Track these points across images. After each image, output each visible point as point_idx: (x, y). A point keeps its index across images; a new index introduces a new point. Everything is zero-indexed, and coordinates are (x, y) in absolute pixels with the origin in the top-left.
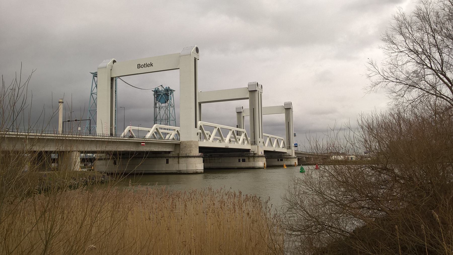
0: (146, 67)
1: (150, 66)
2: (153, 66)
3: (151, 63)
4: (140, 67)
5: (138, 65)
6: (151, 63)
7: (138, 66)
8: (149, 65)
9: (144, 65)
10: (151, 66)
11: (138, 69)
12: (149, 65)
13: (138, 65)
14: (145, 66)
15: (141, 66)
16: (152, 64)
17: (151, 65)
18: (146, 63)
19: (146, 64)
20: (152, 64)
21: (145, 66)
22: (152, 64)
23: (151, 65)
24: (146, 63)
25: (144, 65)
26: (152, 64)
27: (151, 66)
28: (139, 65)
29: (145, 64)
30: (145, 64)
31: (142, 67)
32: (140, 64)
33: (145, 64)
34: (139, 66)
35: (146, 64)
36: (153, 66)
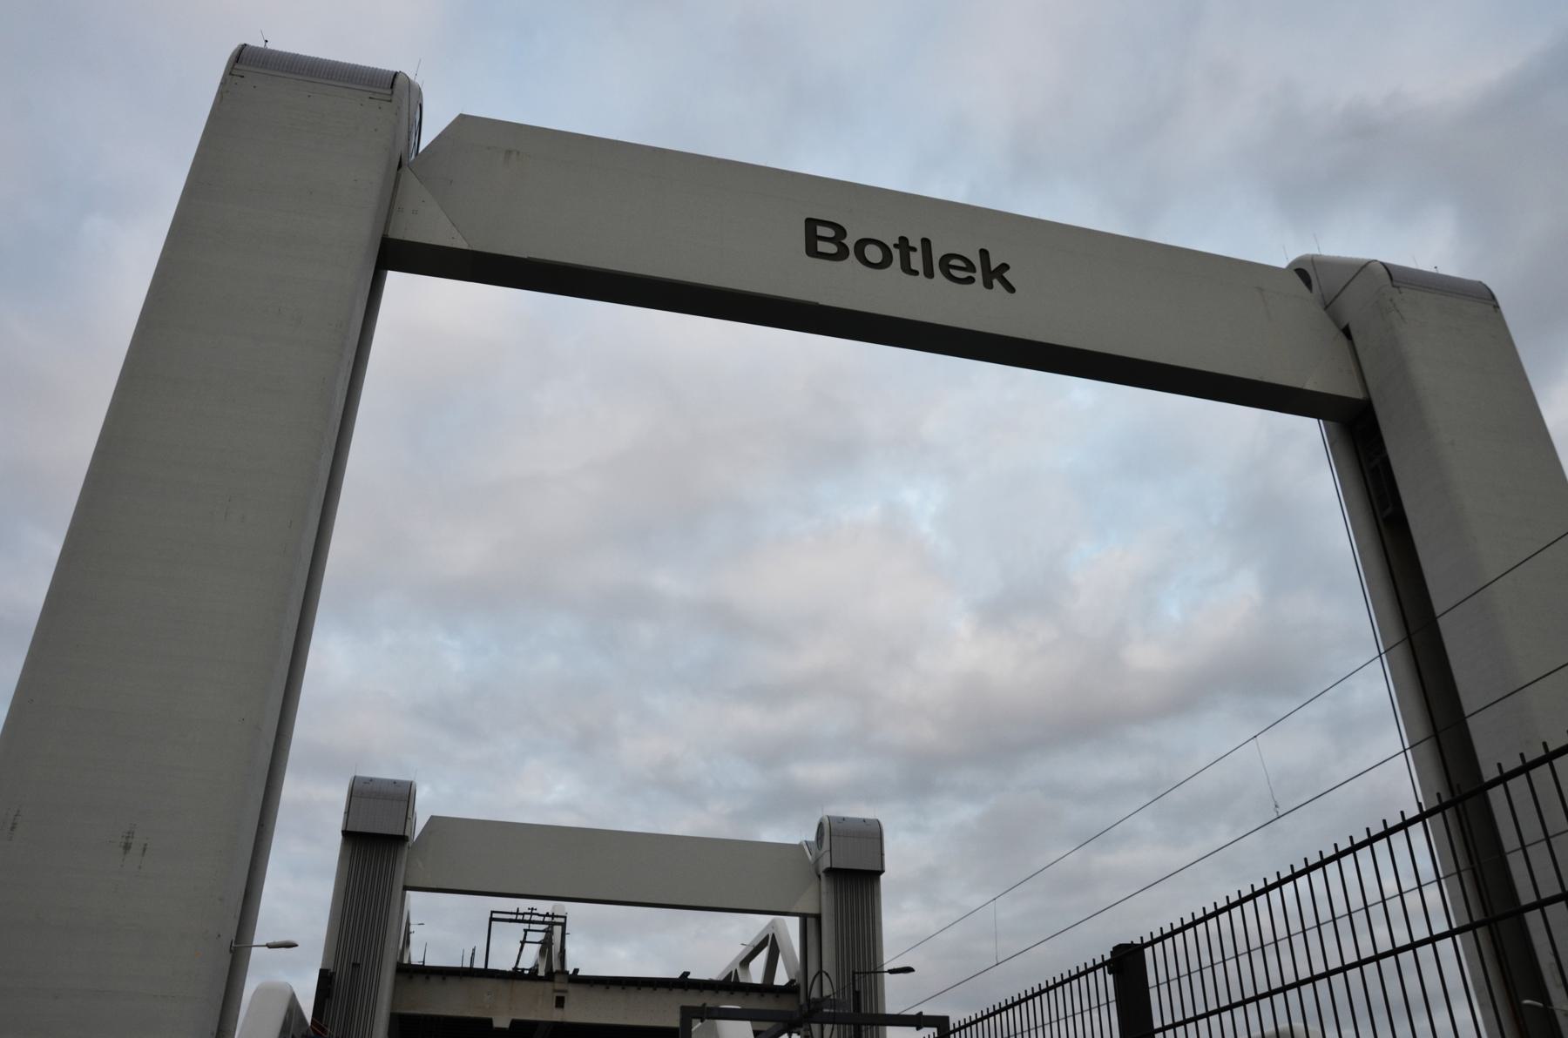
0: (929, 273)
1: (978, 276)
5: (811, 224)
6: (984, 254)
9: (896, 253)
10: (989, 285)
13: (811, 224)
14: (916, 261)
15: (850, 242)
16: (1005, 267)
19: (915, 242)
21: (916, 261)
22: (994, 266)
25: (896, 253)
27: (989, 285)
29: (903, 240)
30: (903, 240)
32: (841, 231)
33: (903, 243)
36: (1011, 289)
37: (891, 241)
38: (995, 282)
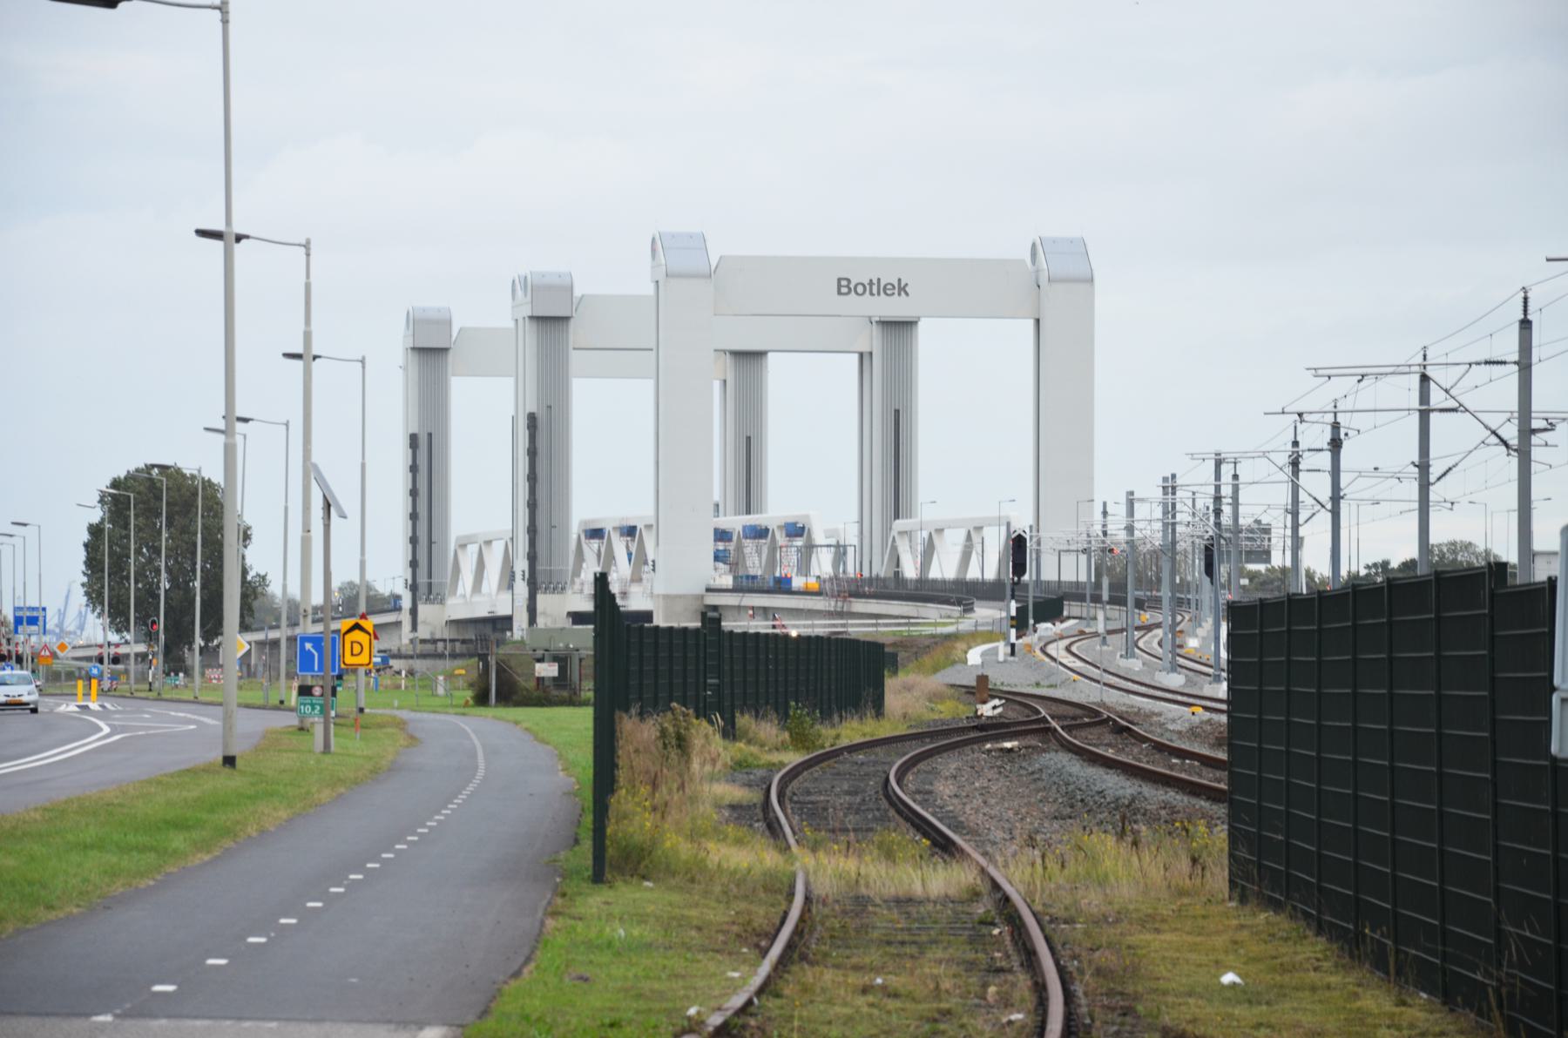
0: (879, 294)
1: (896, 291)
2: (907, 294)
3: (899, 280)
4: (850, 289)
6: (899, 280)
7: (839, 286)
8: (889, 287)
9: (868, 287)
10: (899, 294)
11: (842, 297)
12: (889, 287)
13: (839, 280)
14: (875, 291)
15: (852, 286)
16: (907, 285)
17: (902, 289)
18: (879, 280)
19: (875, 281)
20: (907, 285)
21: (875, 291)
22: (902, 285)
23: (902, 289)
24: (879, 280)
25: (868, 287)
26: (902, 285)
27: (899, 294)
29: (871, 281)
30: (871, 281)
31: (857, 293)
32: (849, 281)
33: (871, 283)
35: (875, 281)
36: (907, 294)
37: (866, 282)
38: (902, 293)
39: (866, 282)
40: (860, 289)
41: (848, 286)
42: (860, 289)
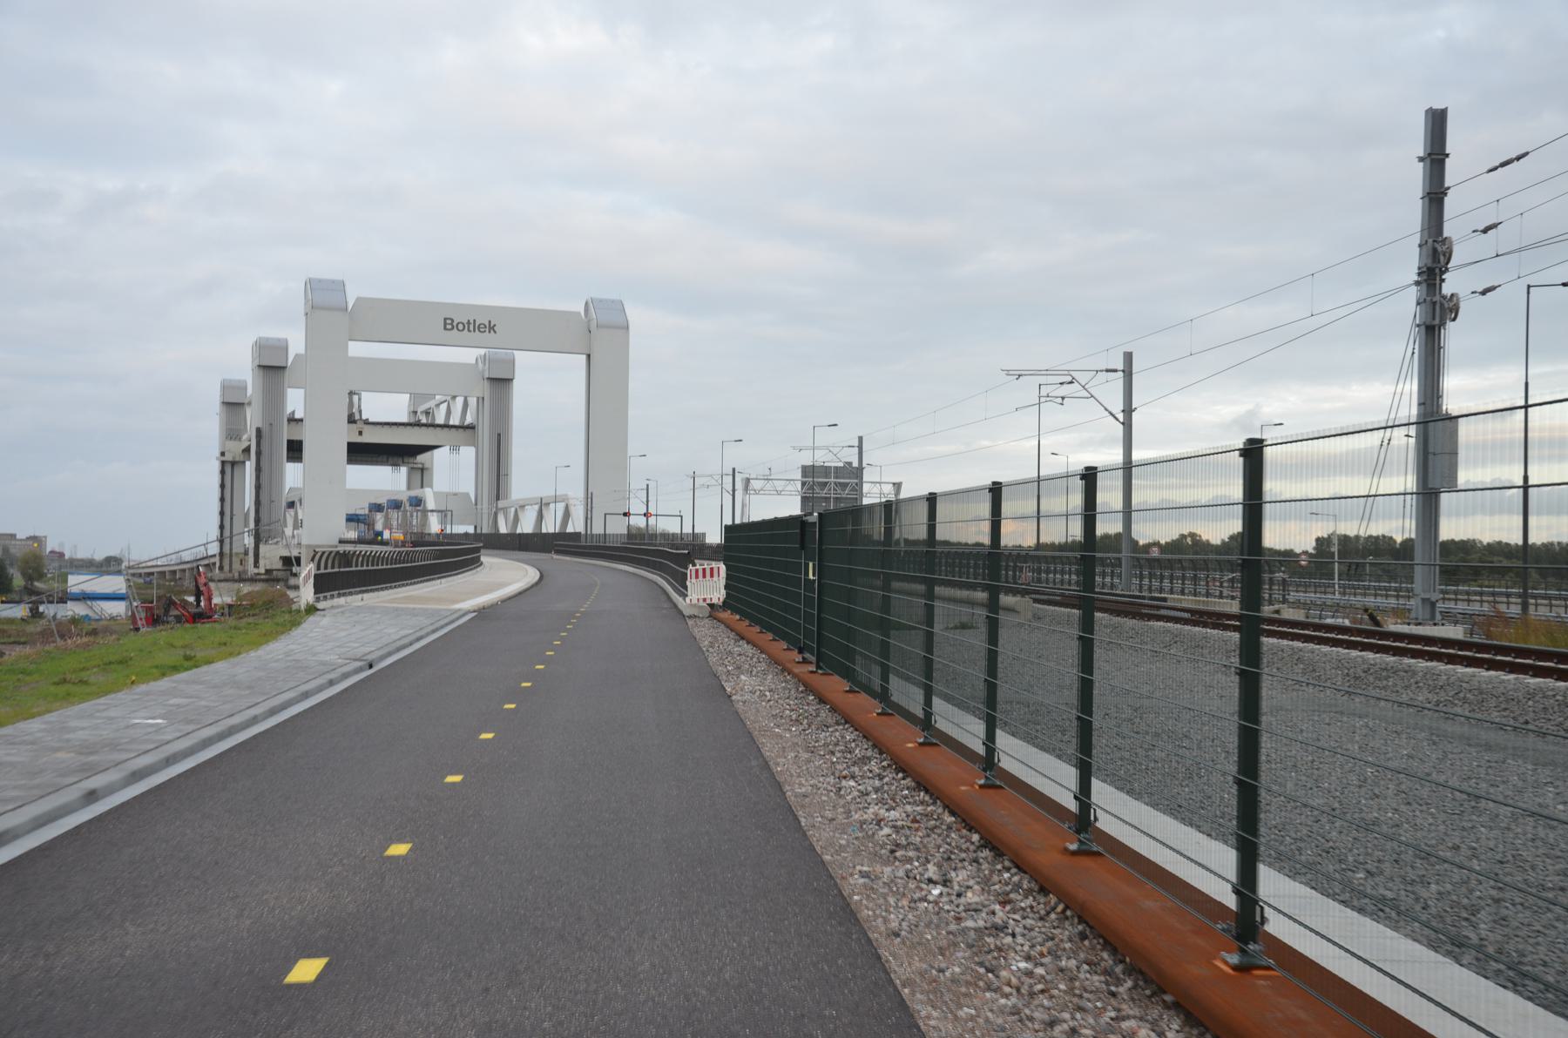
0: (474, 331)
1: (487, 330)
2: (495, 332)
3: (490, 322)
6: (490, 322)
7: (445, 324)
8: (482, 326)
9: (466, 326)
10: (490, 332)
12: (482, 326)
13: (445, 319)
15: (455, 324)
16: (495, 325)
17: (492, 328)
18: (475, 321)
19: (472, 321)
20: (495, 325)
23: (492, 328)
24: (475, 321)
25: (466, 326)
27: (490, 332)
28: (449, 322)
32: (453, 321)
33: (469, 323)
34: (449, 324)
35: (472, 321)
36: (495, 332)
37: (465, 322)
38: (492, 331)
39: (465, 322)
40: (461, 327)
41: (452, 324)
42: (461, 327)
